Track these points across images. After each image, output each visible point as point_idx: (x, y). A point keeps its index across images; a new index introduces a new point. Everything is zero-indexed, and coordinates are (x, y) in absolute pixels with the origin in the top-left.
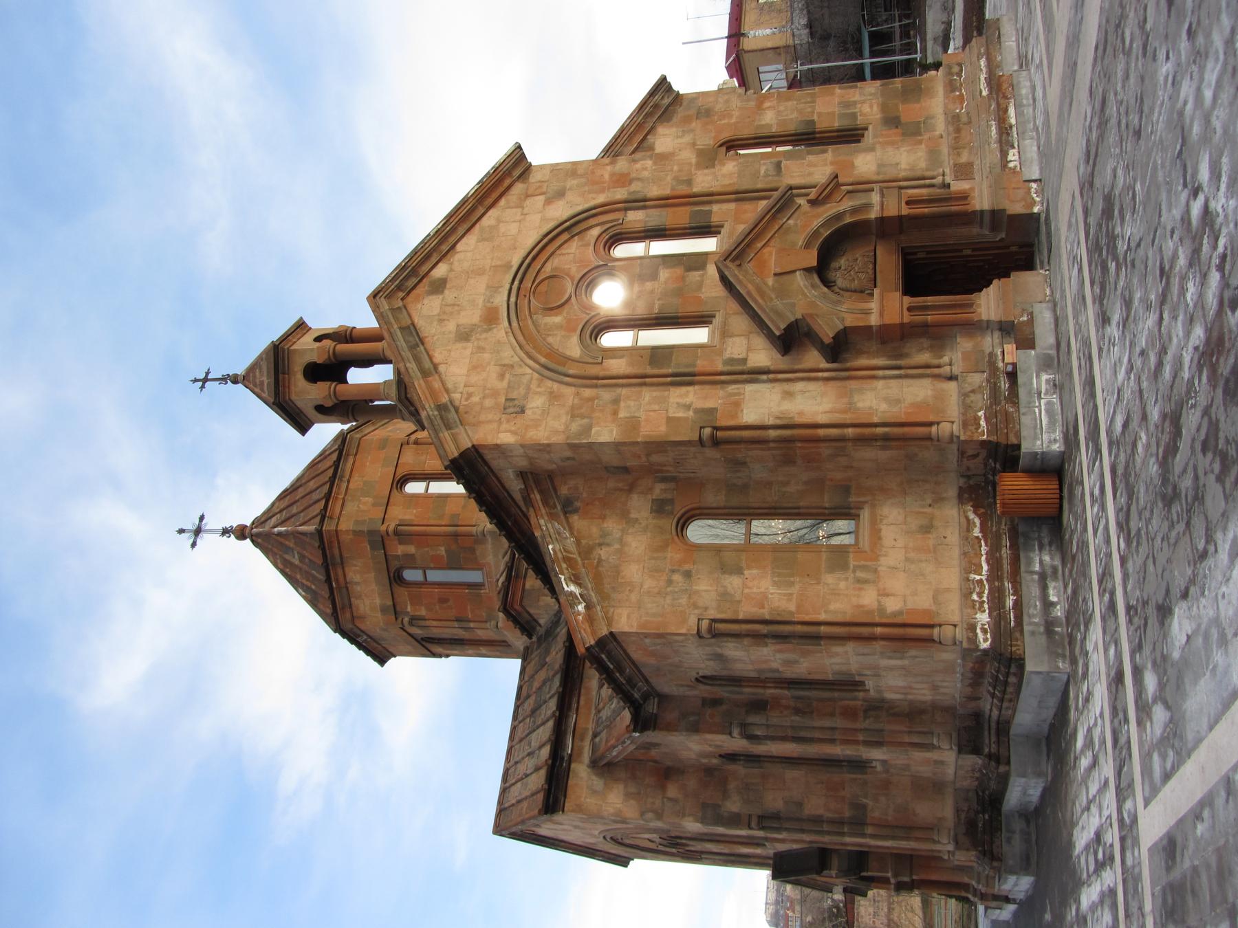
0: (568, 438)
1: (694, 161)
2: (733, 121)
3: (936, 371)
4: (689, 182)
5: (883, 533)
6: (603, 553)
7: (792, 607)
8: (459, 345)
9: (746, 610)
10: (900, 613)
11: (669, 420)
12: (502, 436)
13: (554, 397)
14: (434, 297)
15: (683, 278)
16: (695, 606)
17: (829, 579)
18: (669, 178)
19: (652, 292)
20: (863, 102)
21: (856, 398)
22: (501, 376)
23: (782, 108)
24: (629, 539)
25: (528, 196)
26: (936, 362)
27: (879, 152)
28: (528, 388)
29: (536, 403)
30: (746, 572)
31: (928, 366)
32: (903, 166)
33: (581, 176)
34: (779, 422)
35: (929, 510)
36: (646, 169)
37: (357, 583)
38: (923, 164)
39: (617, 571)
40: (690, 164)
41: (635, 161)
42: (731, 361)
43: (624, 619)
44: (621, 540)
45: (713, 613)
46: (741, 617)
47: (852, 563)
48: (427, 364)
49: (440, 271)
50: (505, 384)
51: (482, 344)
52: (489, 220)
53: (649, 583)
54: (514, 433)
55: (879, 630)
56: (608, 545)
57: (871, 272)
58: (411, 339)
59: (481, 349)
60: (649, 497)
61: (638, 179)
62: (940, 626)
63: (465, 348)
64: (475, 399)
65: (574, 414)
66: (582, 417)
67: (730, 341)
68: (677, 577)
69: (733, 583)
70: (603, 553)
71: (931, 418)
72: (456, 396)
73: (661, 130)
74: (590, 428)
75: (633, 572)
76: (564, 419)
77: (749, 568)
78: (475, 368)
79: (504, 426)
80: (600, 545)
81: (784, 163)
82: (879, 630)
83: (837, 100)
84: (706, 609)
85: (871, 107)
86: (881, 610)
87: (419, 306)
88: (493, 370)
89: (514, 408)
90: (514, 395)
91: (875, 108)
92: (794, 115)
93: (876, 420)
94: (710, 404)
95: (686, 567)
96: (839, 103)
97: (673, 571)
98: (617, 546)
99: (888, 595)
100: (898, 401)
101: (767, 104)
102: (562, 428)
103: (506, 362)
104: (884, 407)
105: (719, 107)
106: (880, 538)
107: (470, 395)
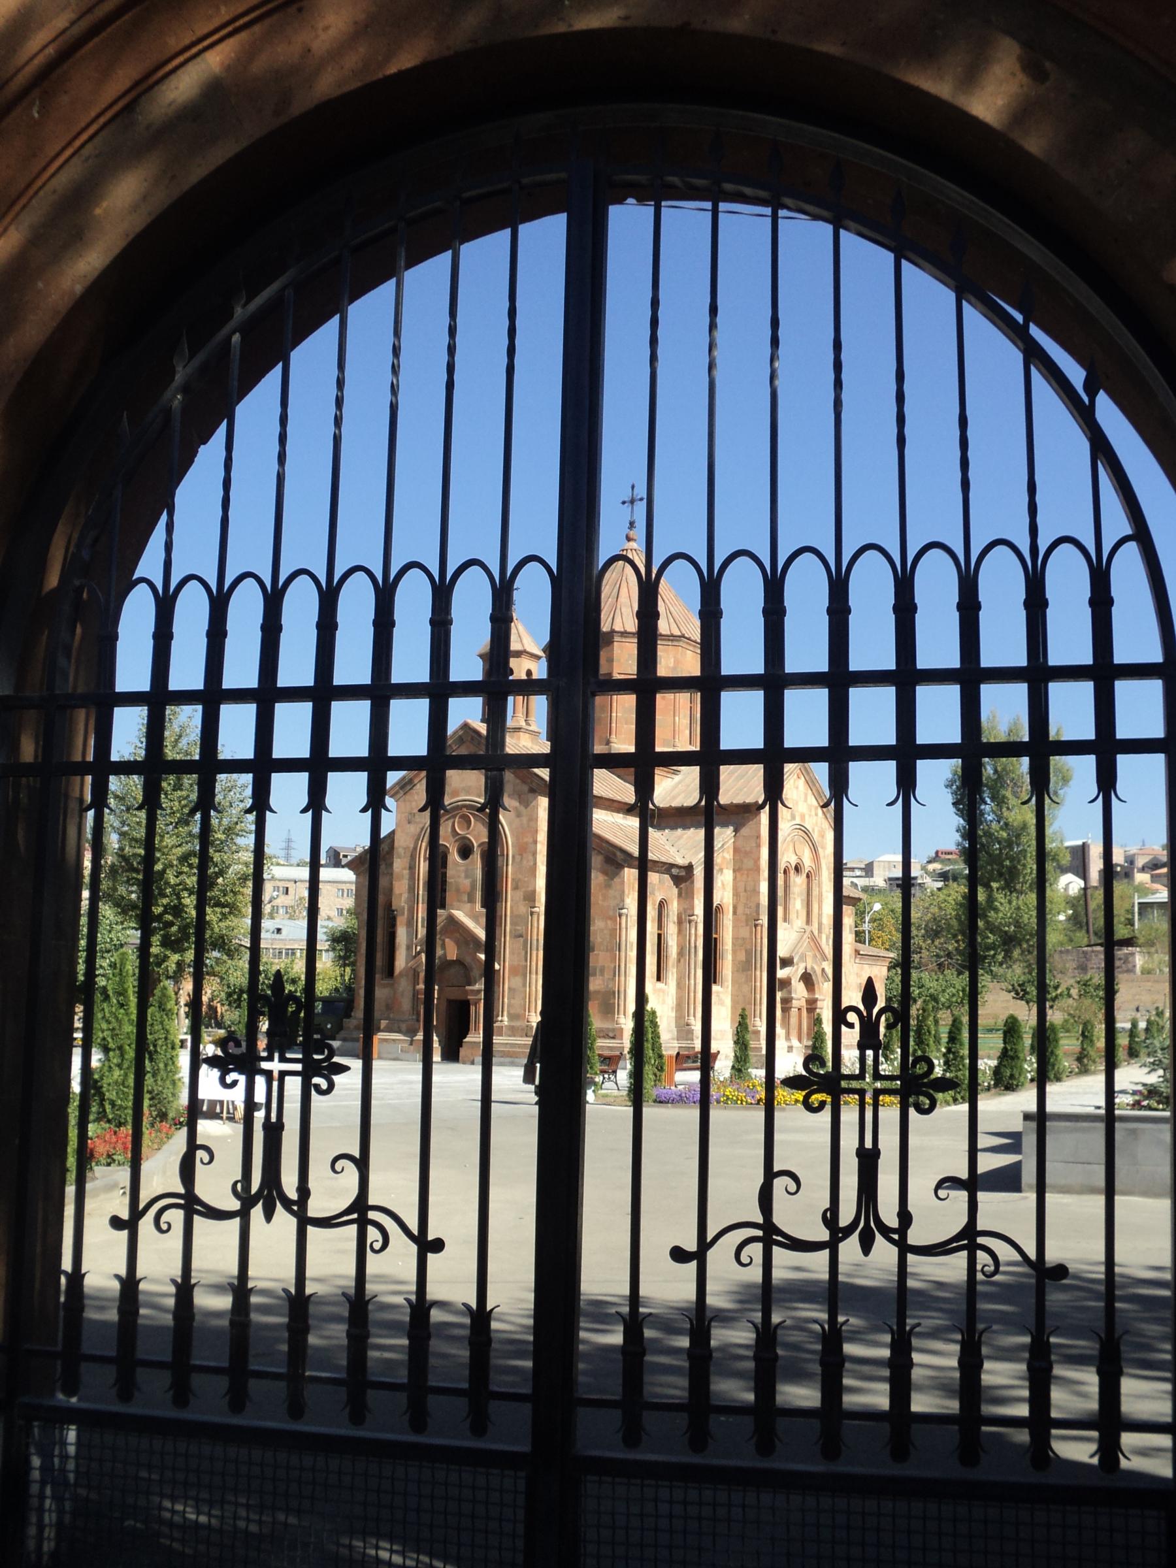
25: (520, 796)
55: (692, 982)
82: (692, 982)
92: (599, 940)
101: (609, 922)
105: (611, 892)
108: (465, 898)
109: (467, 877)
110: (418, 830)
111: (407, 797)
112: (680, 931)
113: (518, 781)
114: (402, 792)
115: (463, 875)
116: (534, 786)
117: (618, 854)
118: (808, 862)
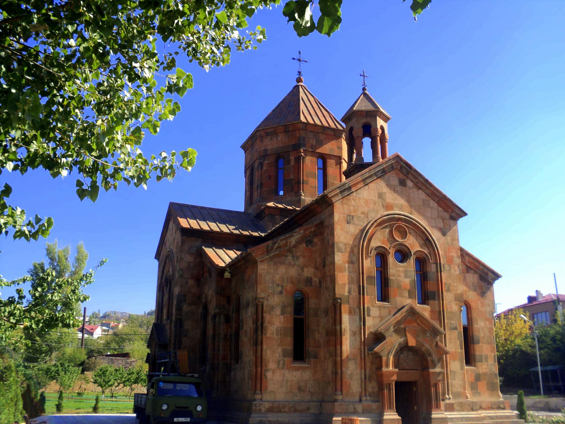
0: (337, 243)
1: (458, 292)
2: (480, 308)
3: (363, 394)
4: (448, 290)
5: (298, 372)
6: (290, 258)
7: (268, 335)
8: (377, 194)
9: (267, 316)
10: (266, 377)
12: (338, 215)
14: (398, 181)
15: (405, 289)
16: (268, 296)
17: (280, 350)
18: (450, 282)
19: (399, 276)
20: (487, 365)
21: (353, 361)
22: (363, 213)
23: (485, 329)
24: (295, 268)
25: (443, 220)
26: (367, 394)
27: (460, 371)
28: (358, 225)
30: (282, 316)
31: (365, 390)
32: (454, 382)
33: (452, 243)
34: (343, 330)
35: (308, 390)
36: (455, 271)
37: (277, 139)
38: (454, 390)
39: (283, 263)
40: (457, 290)
41: (459, 266)
42: (369, 309)
43: (263, 267)
44: (295, 264)
45: (265, 303)
46: (264, 314)
47: (286, 359)
48: (368, 181)
49: (410, 183)
50: (360, 215)
51: (377, 204)
52: (433, 204)
53: (277, 277)
54: (339, 219)
56: (293, 260)
57: (407, 368)
58: (380, 173)
59: (375, 203)
60: (313, 276)
61: (450, 268)
62: (261, 394)
63: (375, 197)
64: (353, 202)
66: (345, 249)
67: (378, 309)
68: (280, 288)
69: (278, 311)
70: (290, 258)
71: (344, 392)
72: (354, 194)
73: (476, 276)
74: (341, 252)
75: (282, 270)
76: (345, 241)
77: (284, 317)
78: (367, 201)
79: (342, 216)
80: (293, 256)
81: (456, 332)
83: (489, 354)
84: (267, 300)
85: (485, 369)
86: (267, 370)
87: (394, 175)
88: (366, 210)
89: (349, 220)
90: (355, 218)
91: (485, 371)
92: (482, 335)
93: (344, 369)
95: (284, 292)
96: (487, 355)
97: (282, 286)
98: (292, 263)
99: (273, 373)
100: (351, 378)
101: (487, 323)
102: (341, 240)
103: (369, 215)
104: (349, 372)
105: (486, 301)
106: (296, 370)
107: (355, 200)
108: (406, 294)
109: (406, 276)
110: (357, 231)
111: (345, 200)
113: (440, 209)
115: (403, 274)
116: (454, 215)
117: (491, 274)
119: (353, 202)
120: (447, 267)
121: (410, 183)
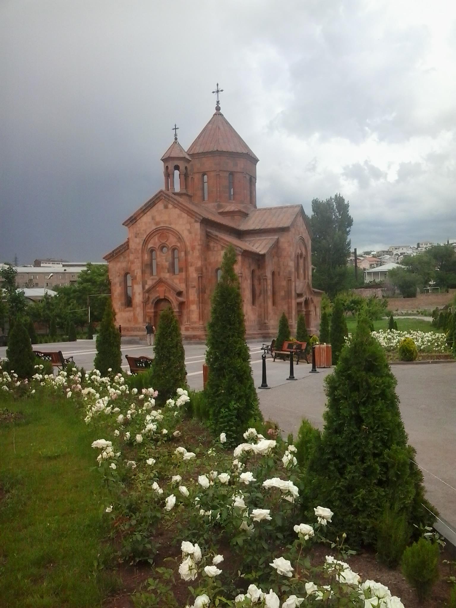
4: (191, 266)
11: (134, 270)
13: (139, 244)
22: (143, 230)
29: (137, 240)
38: (192, 320)
42: (146, 281)
49: (170, 206)
52: (184, 215)
65: (136, 249)
94: (138, 278)
108: (167, 271)
109: (166, 261)
112: (260, 284)
114: (131, 224)
115: (164, 260)
118: (304, 253)
119: (139, 226)
120: (191, 252)
121: (170, 206)
